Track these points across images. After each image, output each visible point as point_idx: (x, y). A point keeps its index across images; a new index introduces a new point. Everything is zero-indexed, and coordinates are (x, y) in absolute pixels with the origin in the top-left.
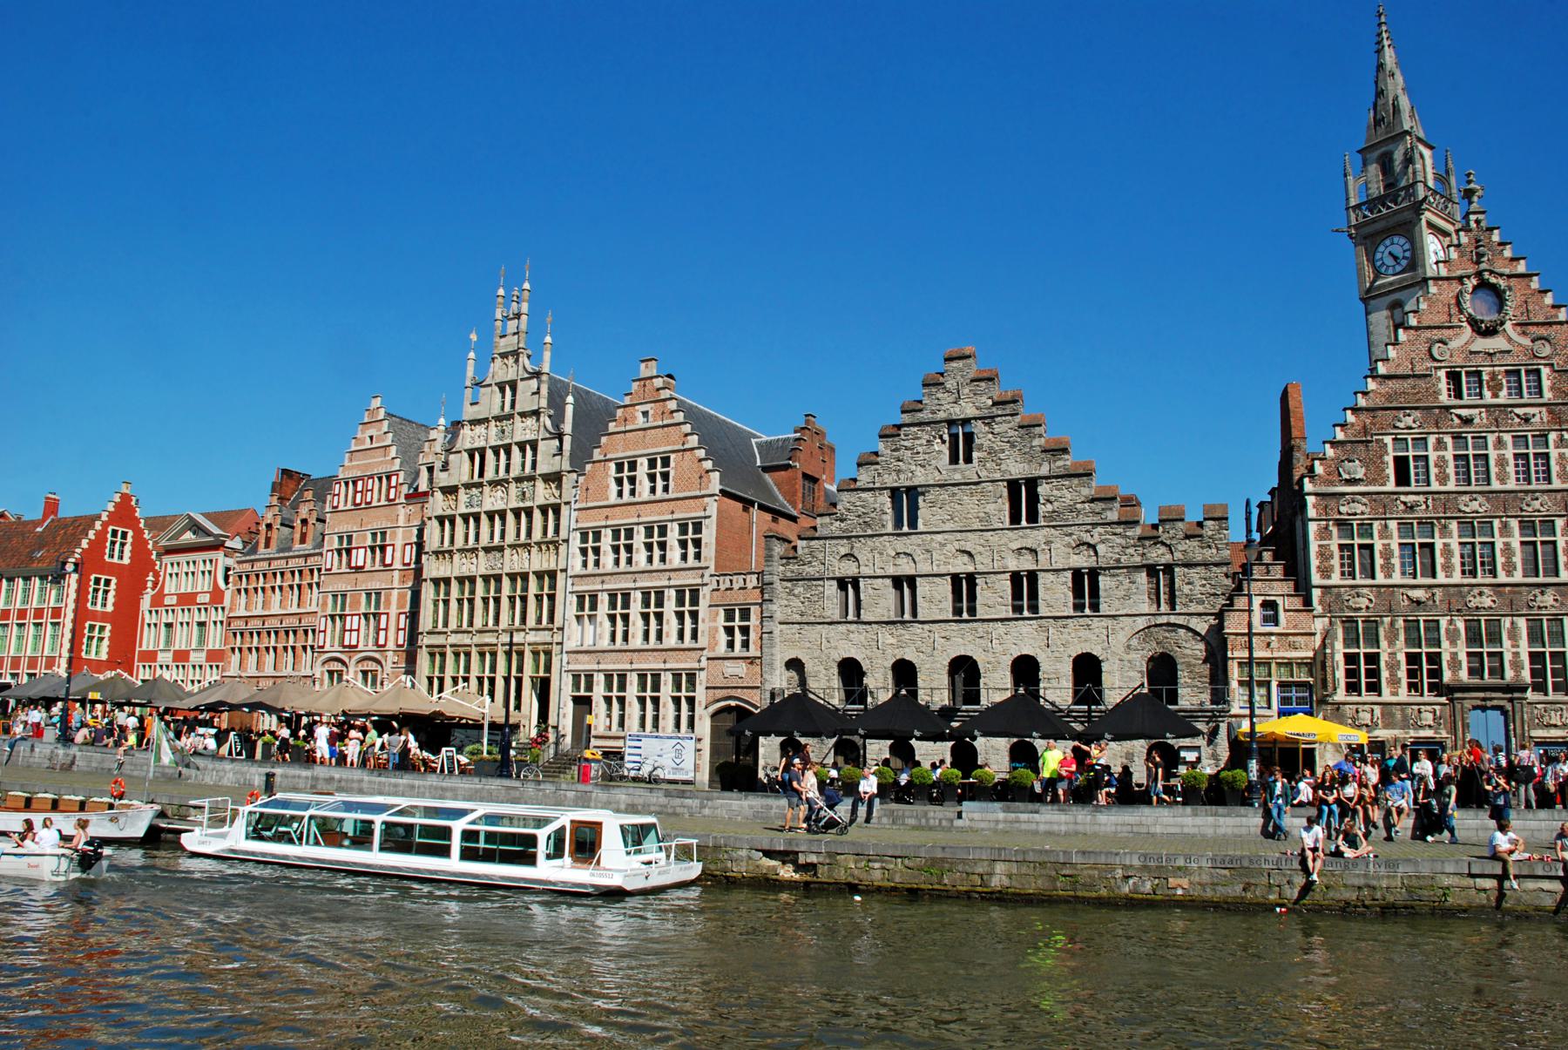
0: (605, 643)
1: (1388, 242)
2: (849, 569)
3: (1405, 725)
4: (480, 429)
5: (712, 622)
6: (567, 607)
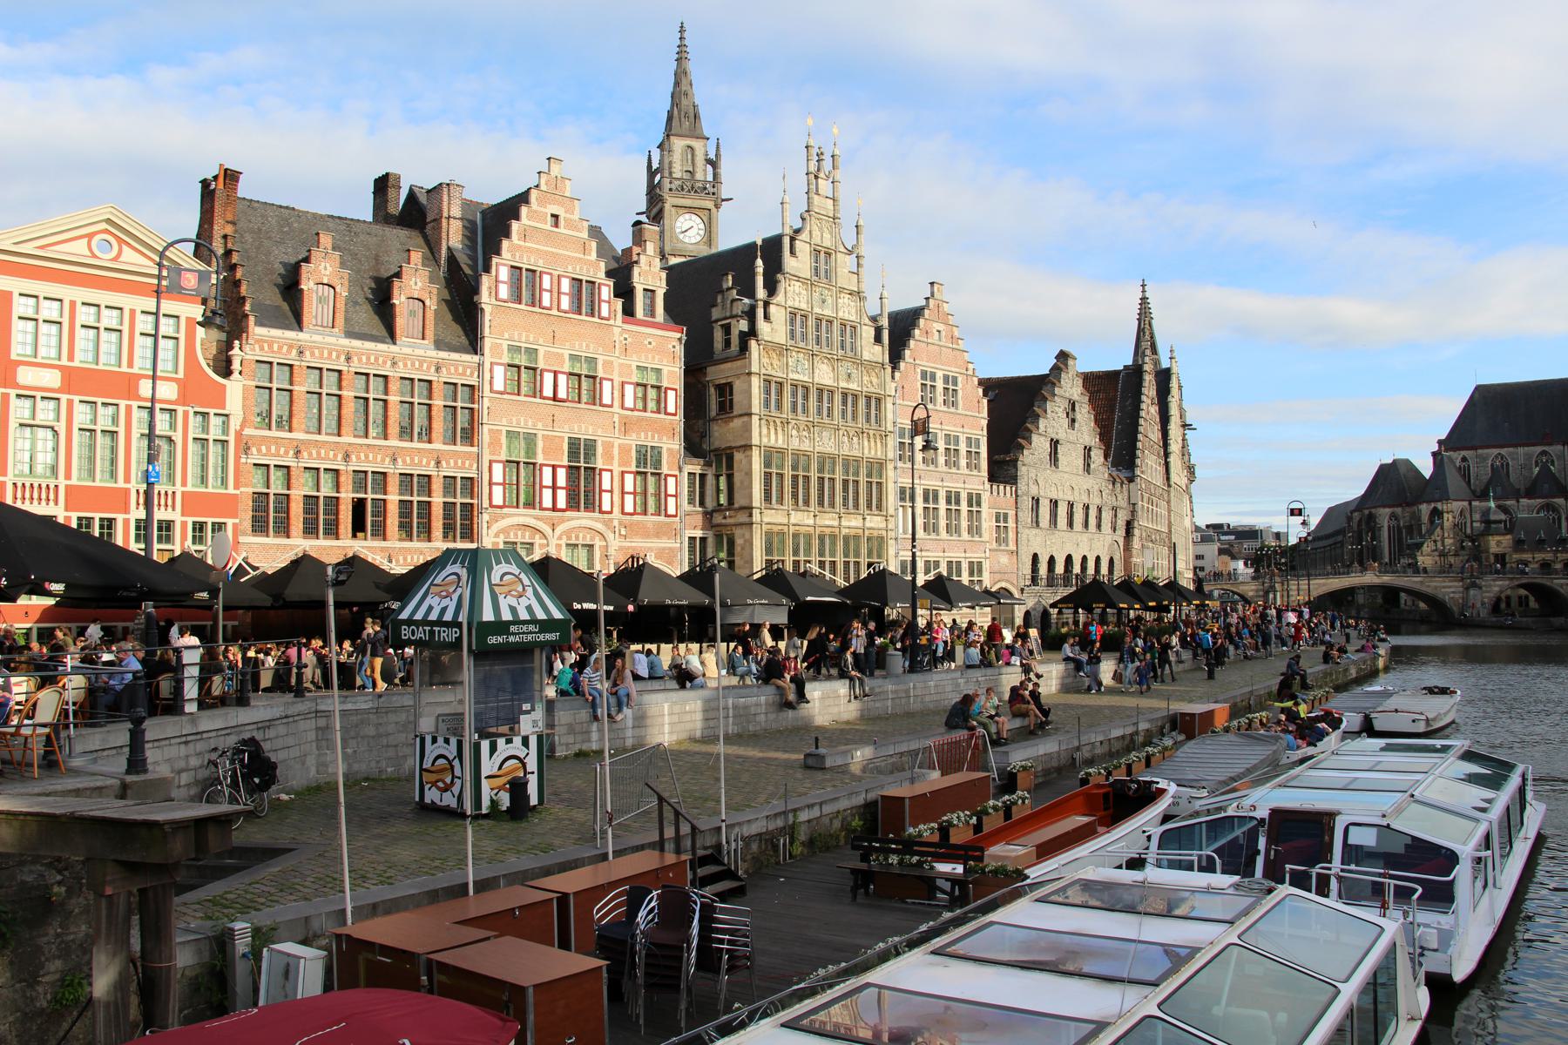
2: (1034, 491)
5: (988, 524)
6: (891, 498)
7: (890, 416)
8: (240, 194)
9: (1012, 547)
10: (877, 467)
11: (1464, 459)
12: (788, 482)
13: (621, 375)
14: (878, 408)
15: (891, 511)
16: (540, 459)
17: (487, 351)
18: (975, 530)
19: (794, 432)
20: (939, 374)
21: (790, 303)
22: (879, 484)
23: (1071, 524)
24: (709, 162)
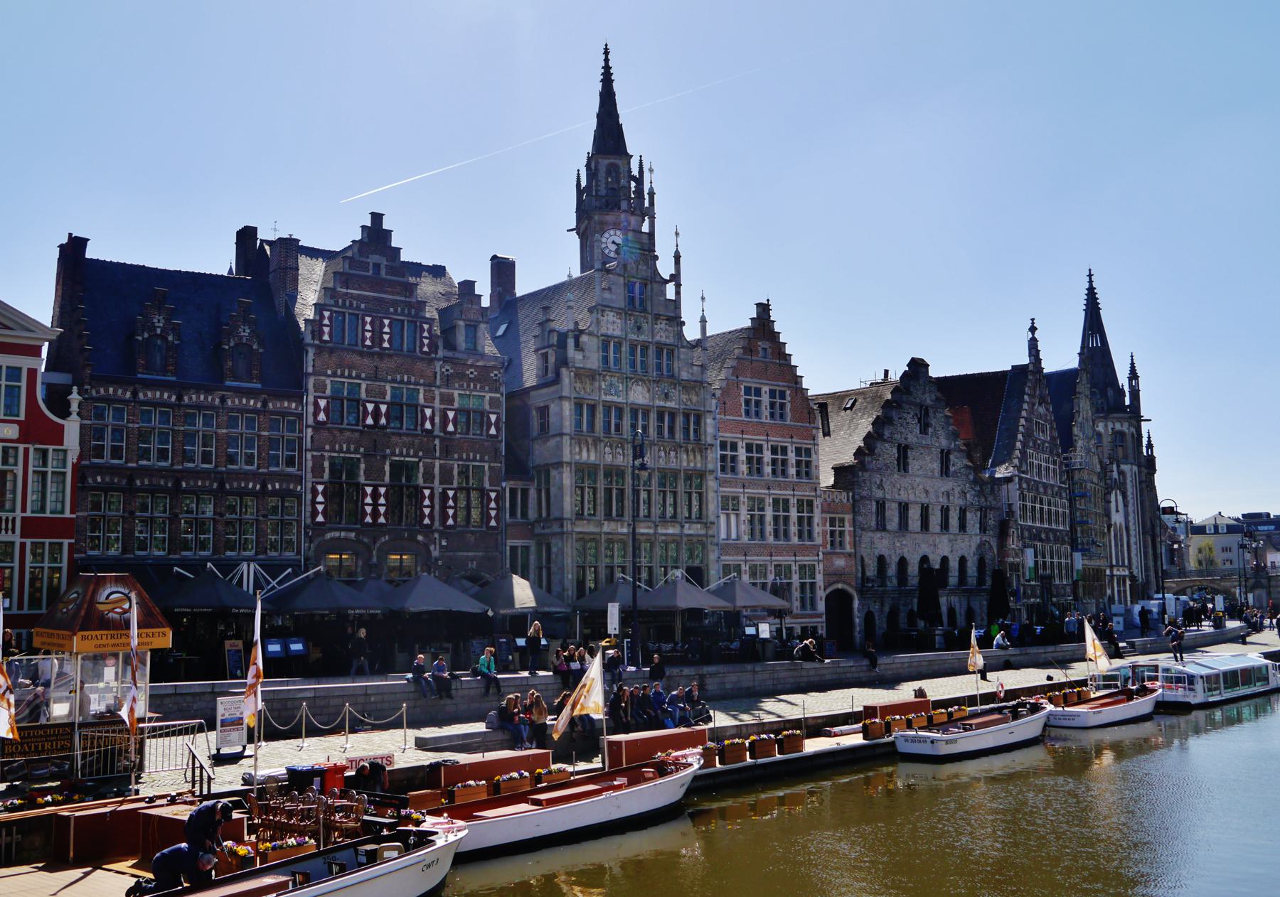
0: (745, 539)
1: (612, 232)
2: (879, 494)
3: (1036, 597)
4: (610, 316)
5: (820, 528)
6: (712, 506)
7: (710, 430)
8: (87, 256)
9: (848, 549)
12: (601, 495)
13: (442, 402)
14: (698, 423)
15: (712, 518)
16: (362, 480)
17: (311, 386)
19: (607, 449)
20: (765, 389)
21: (603, 331)
22: (700, 494)
23: (925, 525)
24: (634, 178)
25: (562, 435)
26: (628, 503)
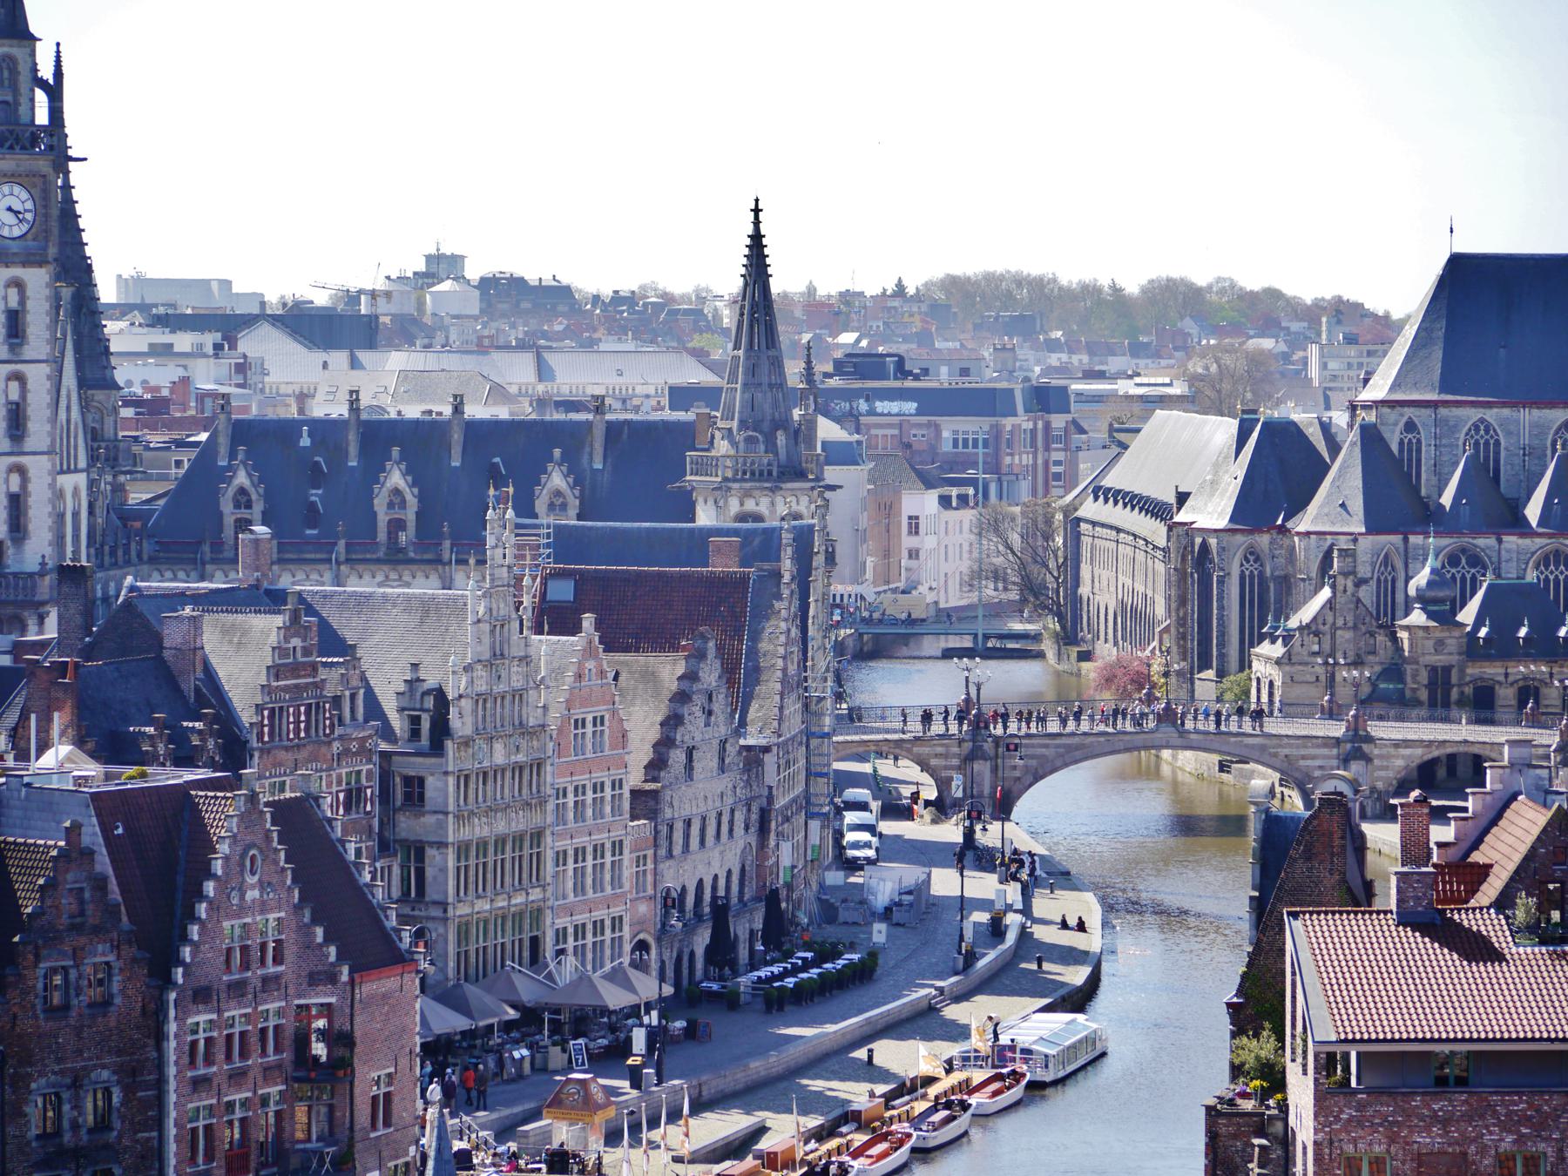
5: (628, 870)
7: (549, 779)
10: (538, 836)
11: (1410, 426)
12: (472, 872)
15: (549, 879)
18: (616, 881)
24: (43, 84)
25: (446, 813)
26: (490, 876)
